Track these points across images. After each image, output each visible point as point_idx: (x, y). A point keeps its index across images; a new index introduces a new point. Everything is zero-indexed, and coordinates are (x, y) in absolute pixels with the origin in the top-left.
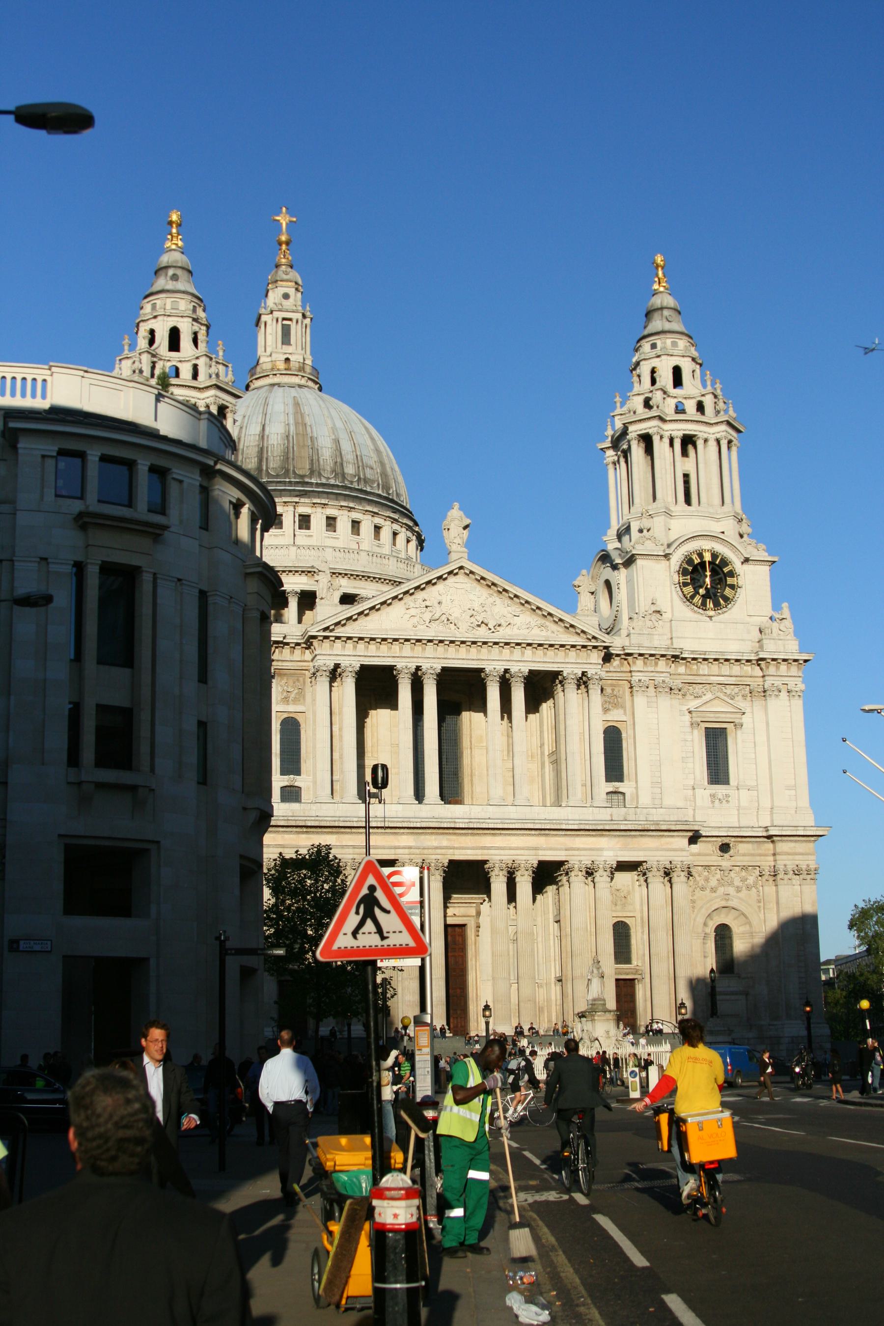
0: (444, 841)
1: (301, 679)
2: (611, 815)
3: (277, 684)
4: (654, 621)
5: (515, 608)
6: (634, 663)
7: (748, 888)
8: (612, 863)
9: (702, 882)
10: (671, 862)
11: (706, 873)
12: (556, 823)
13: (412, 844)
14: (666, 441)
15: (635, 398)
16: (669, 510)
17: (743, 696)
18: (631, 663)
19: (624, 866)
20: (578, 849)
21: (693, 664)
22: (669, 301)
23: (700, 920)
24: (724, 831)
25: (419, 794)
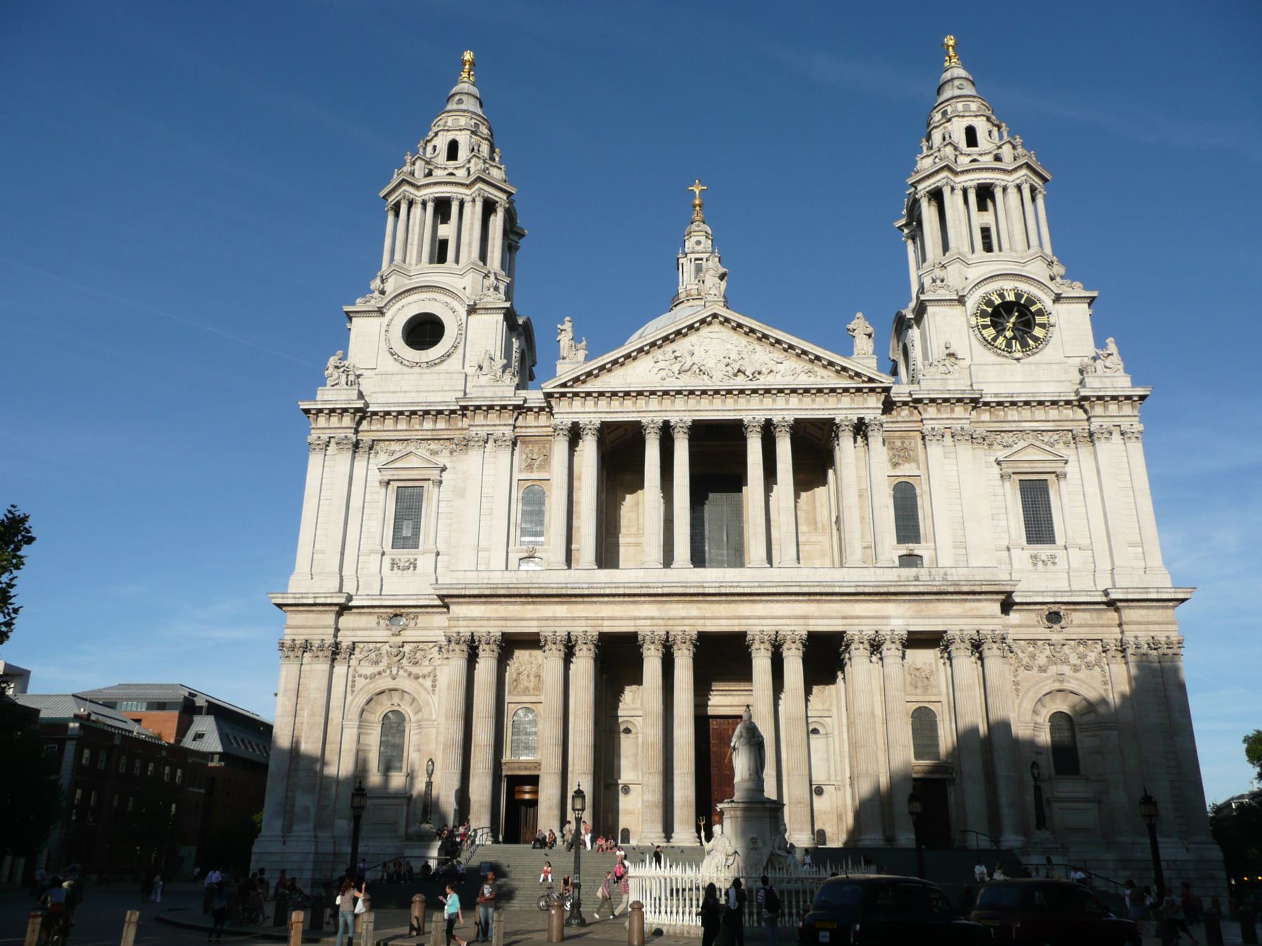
0: (693, 610)
1: (547, 446)
2: (899, 576)
3: (521, 452)
4: (948, 366)
5: (778, 354)
6: (925, 410)
7: (1089, 666)
8: (901, 633)
9: (1026, 660)
10: (978, 632)
11: (1031, 649)
12: (827, 586)
13: (656, 614)
14: (959, 193)
15: (924, 161)
16: (965, 256)
17: (1065, 443)
18: (921, 411)
19: (916, 640)
20: (858, 617)
21: (999, 410)
22: (961, 72)
23: (1028, 705)
24: (1050, 596)
25: (668, 560)
